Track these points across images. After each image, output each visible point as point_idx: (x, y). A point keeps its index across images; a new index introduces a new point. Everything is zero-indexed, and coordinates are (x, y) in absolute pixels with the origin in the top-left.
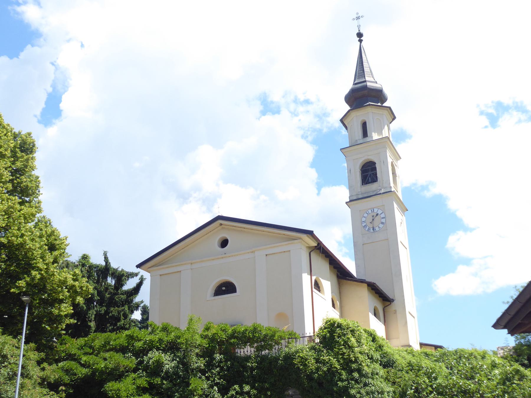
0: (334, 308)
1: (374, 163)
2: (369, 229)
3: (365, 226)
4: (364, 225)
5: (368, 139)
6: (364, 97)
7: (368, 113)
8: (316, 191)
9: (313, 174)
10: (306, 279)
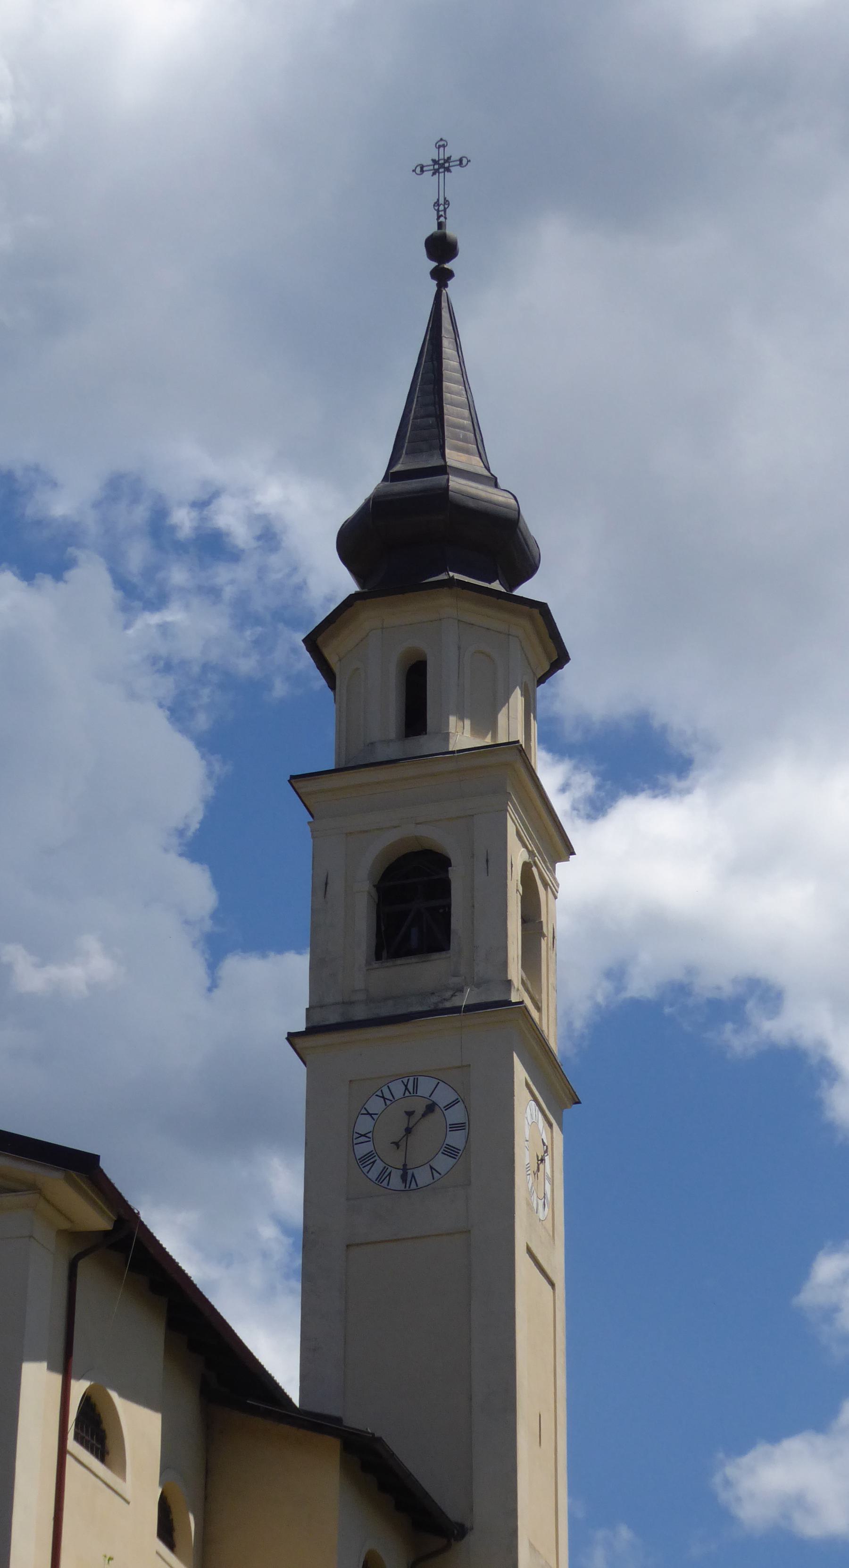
0: (171, 1544)
1: (444, 862)
2: (384, 1175)
3: (367, 1160)
4: (363, 1149)
5: (426, 744)
6: (435, 544)
7: (441, 623)
8: (200, 971)
9: (196, 888)
10: (39, 1389)
